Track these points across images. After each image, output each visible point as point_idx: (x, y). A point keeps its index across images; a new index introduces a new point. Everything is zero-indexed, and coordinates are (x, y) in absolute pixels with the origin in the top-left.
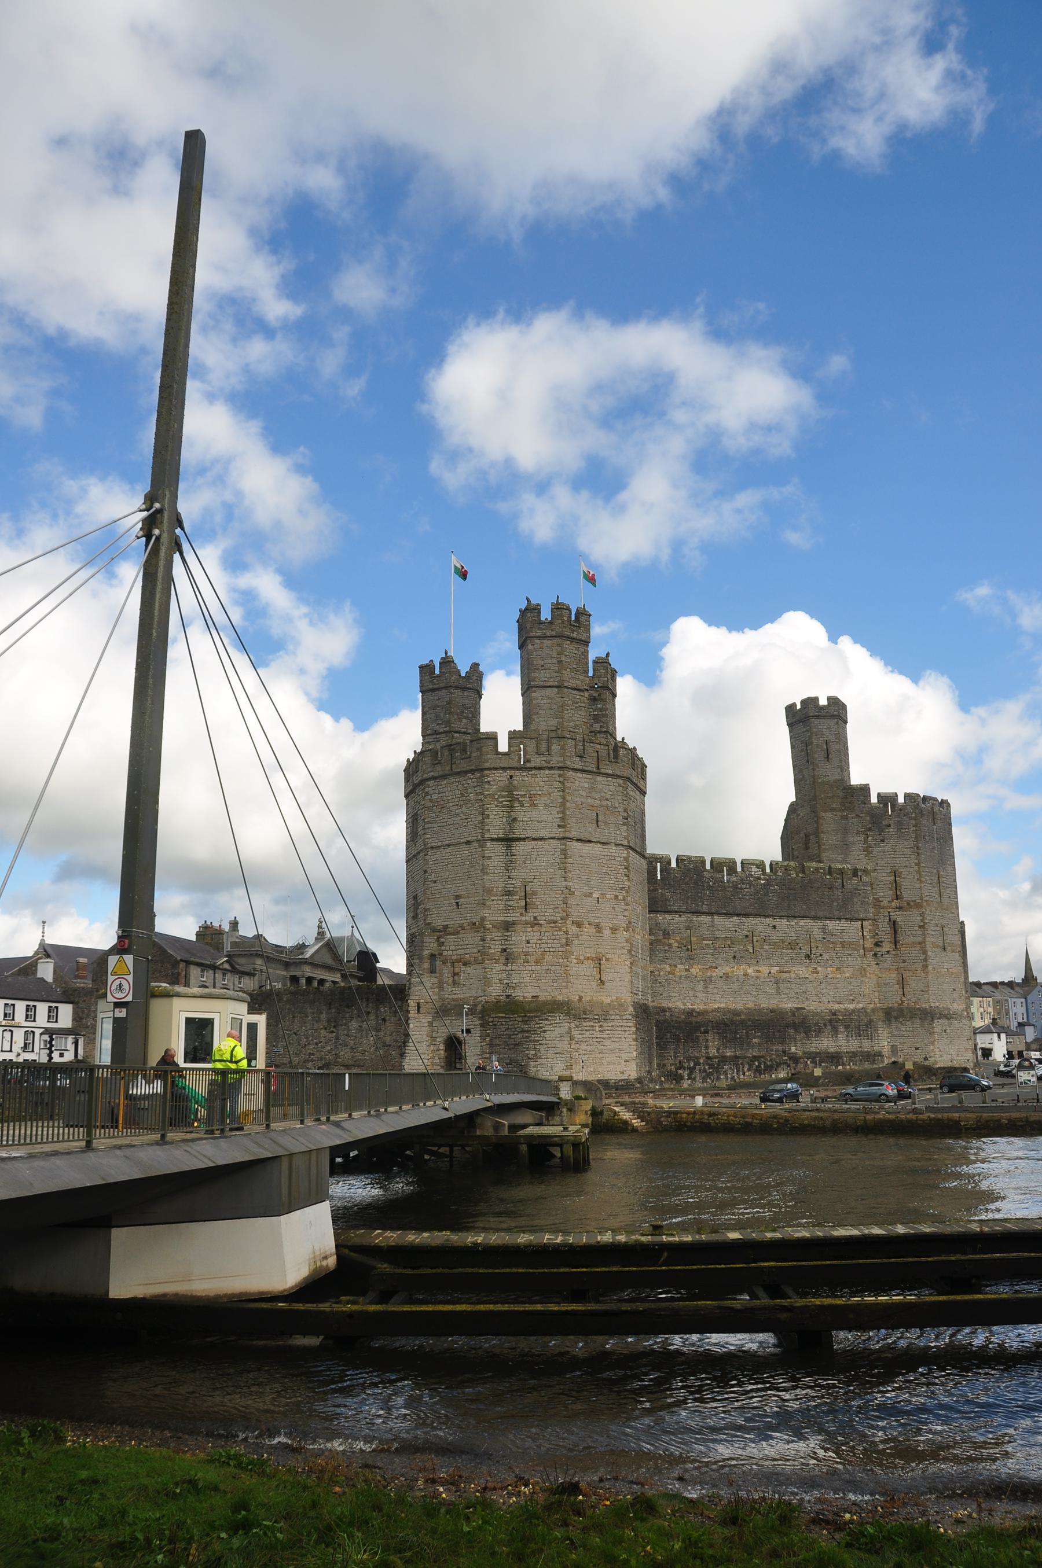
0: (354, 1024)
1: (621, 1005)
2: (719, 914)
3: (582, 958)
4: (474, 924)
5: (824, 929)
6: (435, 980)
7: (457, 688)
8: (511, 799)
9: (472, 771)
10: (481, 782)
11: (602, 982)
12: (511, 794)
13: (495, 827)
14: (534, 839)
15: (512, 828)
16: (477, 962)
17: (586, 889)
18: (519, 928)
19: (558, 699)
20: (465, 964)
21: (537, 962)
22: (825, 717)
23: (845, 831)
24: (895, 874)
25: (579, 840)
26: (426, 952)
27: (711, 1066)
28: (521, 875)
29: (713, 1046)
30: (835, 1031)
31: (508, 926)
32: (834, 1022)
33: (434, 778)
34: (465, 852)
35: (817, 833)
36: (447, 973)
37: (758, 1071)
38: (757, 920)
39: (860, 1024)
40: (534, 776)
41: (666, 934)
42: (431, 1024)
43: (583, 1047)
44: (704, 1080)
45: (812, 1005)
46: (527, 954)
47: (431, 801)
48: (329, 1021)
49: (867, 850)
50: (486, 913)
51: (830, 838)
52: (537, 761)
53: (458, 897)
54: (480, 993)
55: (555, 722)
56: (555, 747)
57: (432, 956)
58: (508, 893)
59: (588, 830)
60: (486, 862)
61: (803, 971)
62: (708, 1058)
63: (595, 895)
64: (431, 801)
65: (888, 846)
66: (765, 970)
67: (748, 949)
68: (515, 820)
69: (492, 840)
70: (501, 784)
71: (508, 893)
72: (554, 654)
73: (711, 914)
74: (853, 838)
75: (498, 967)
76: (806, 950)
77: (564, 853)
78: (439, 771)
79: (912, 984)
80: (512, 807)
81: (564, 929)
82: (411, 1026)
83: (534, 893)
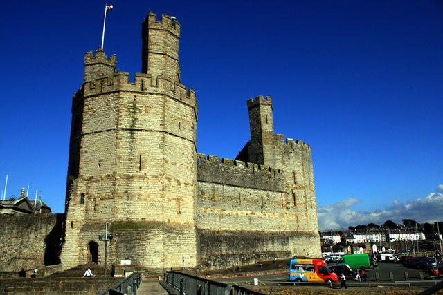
0: (32, 235)
1: (189, 226)
2: (226, 185)
3: (170, 198)
4: (109, 176)
5: (268, 195)
6: (84, 209)
7: (104, 64)
8: (134, 108)
9: (114, 92)
10: (118, 97)
11: (179, 212)
12: (134, 105)
13: (125, 122)
14: (147, 131)
15: (133, 125)
16: (110, 198)
17: (173, 161)
19: (164, 60)
20: (102, 199)
21: (145, 199)
22: (265, 105)
23: (274, 153)
24: (294, 173)
25: (171, 134)
26: (79, 192)
27: (223, 259)
28: (138, 150)
29: (224, 249)
30: (273, 242)
31: (129, 178)
32: (273, 237)
33: (91, 96)
34: (106, 135)
35: (262, 154)
36: (90, 204)
37: (243, 261)
38: (242, 189)
39: (284, 238)
40: (148, 97)
41: (203, 193)
42: (79, 234)
43: (171, 248)
44: (220, 266)
45: (265, 230)
46: (139, 194)
47: (89, 109)
48: (17, 233)
49: (283, 162)
50: (117, 170)
51: (268, 154)
52: (150, 90)
53: (100, 161)
54: (111, 216)
55: (161, 71)
56: (160, 84)
57: (83, 195)
58: (130, 159)
59: (175, 130)
60: (119, 141)
61: (259, 214)
62: (222, 255)
63: (178, 165)
64: (89, 109)
65: (291, 161)
66: (245, 212)
67: (238, 202)
68: (136, 119)
69: (123, 129)
70: (130, 100)
71: (130, 159)
72: (162, 38)
73: (223, 184)
76: (261, 205)
77: (163, 140)
78: (94, 92)
79: (302, 222)
80: (135, 112)
81: (161, 181)
82: (67, 235)
83: (146, 160)
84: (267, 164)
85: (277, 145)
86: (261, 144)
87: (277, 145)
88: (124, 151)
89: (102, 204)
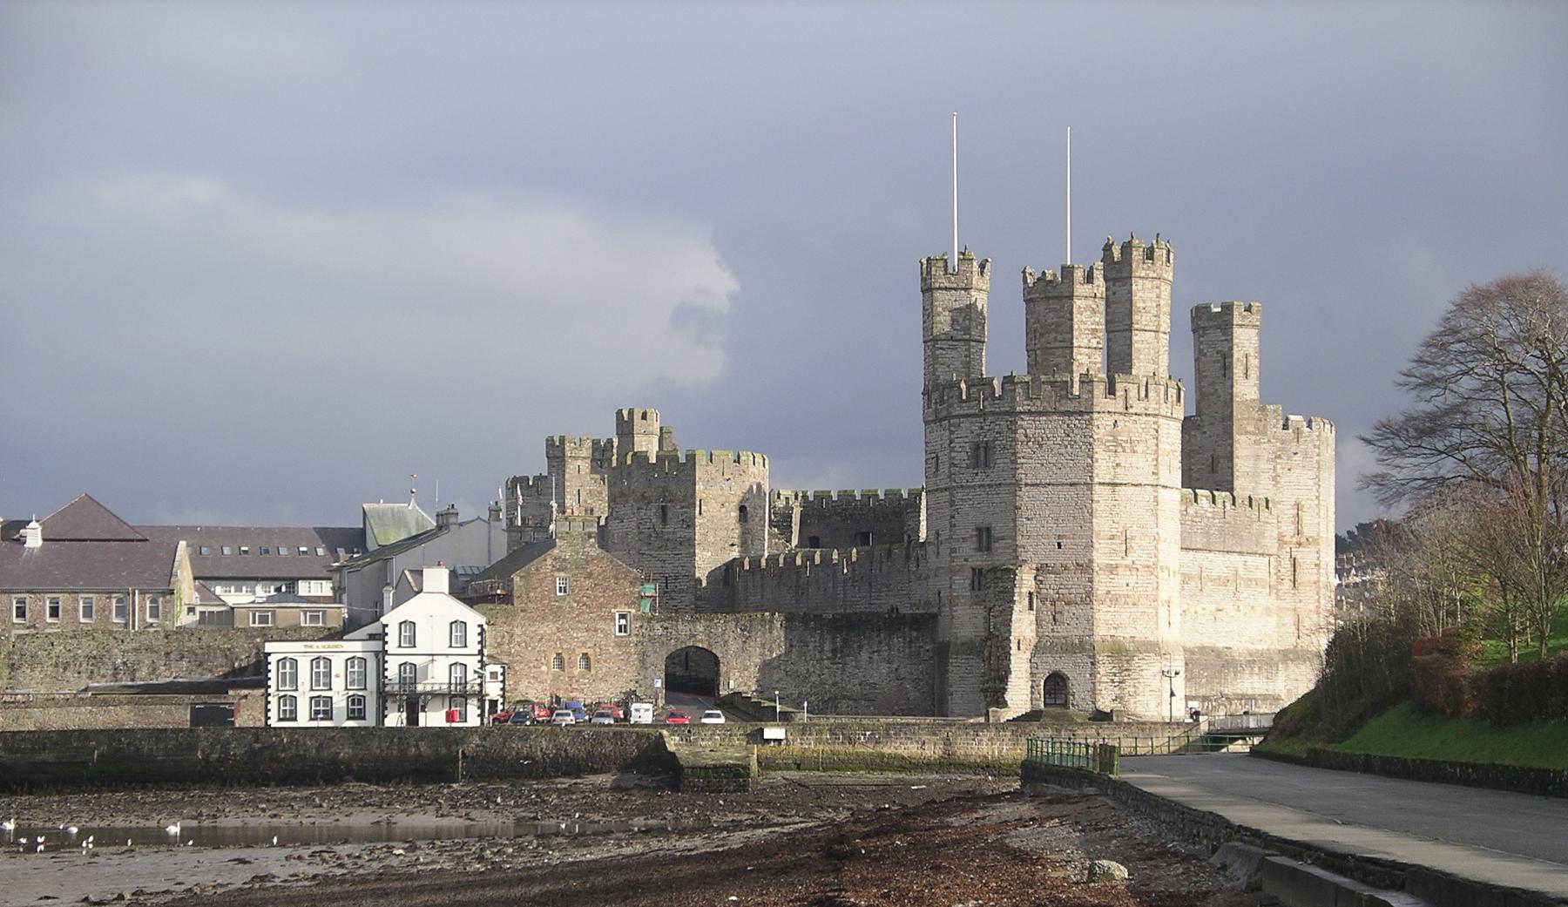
0: (864, 656)
9: (1081, 413)
18: (1120, 570)
24: (1298, 506)
30: (1252, 674)
31: (1113, 569)
33: (1030, 413)
35: (1230, 457)
36: (1047, 609)
48: (834, 651)
49: (1275, 479)
58: (1113, 537)
65: (1293, 476)
71: (1113, 537)
74: (1263, 465)
75: (1103, 608)
84: (1242, 485)
85: (1264, 434)
86: (1228, 433)
87: (1264, 434)
88: (1101, 524)
89: (1068, 612)
